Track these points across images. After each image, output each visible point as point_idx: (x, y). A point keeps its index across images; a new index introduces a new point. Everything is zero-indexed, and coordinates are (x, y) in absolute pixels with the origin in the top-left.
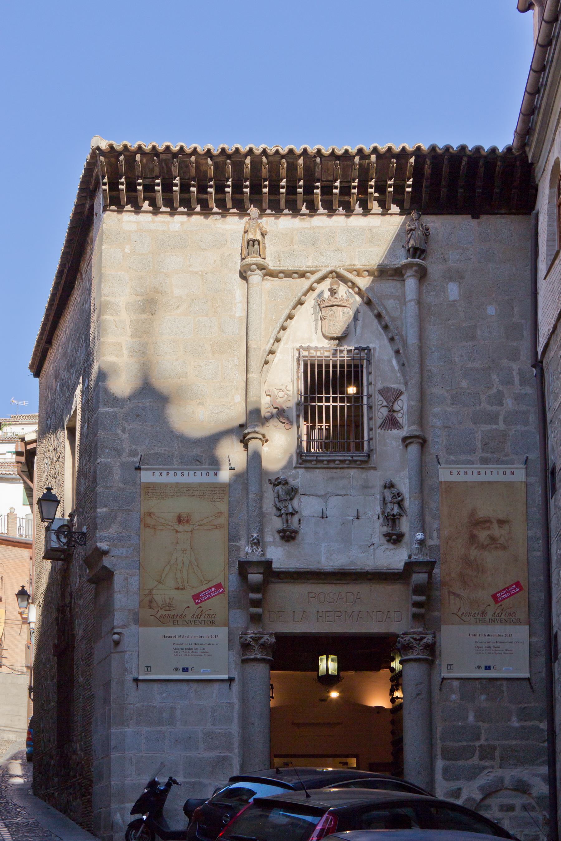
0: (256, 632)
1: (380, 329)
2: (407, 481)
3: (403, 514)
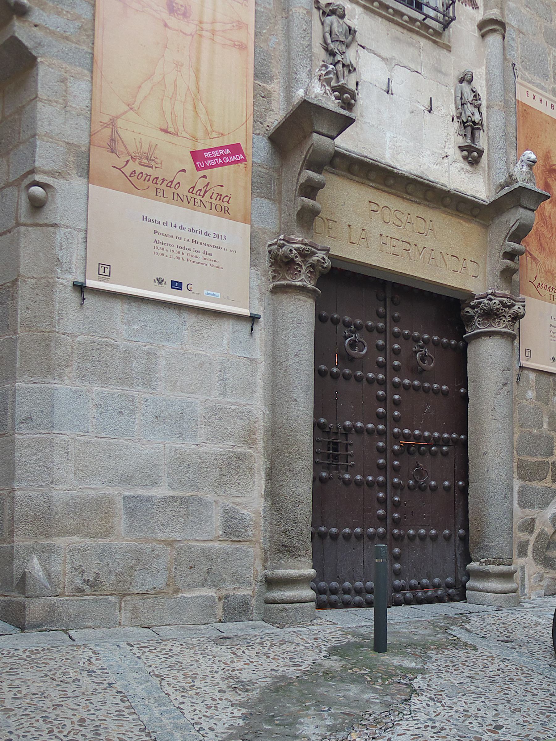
0: (306, 241)
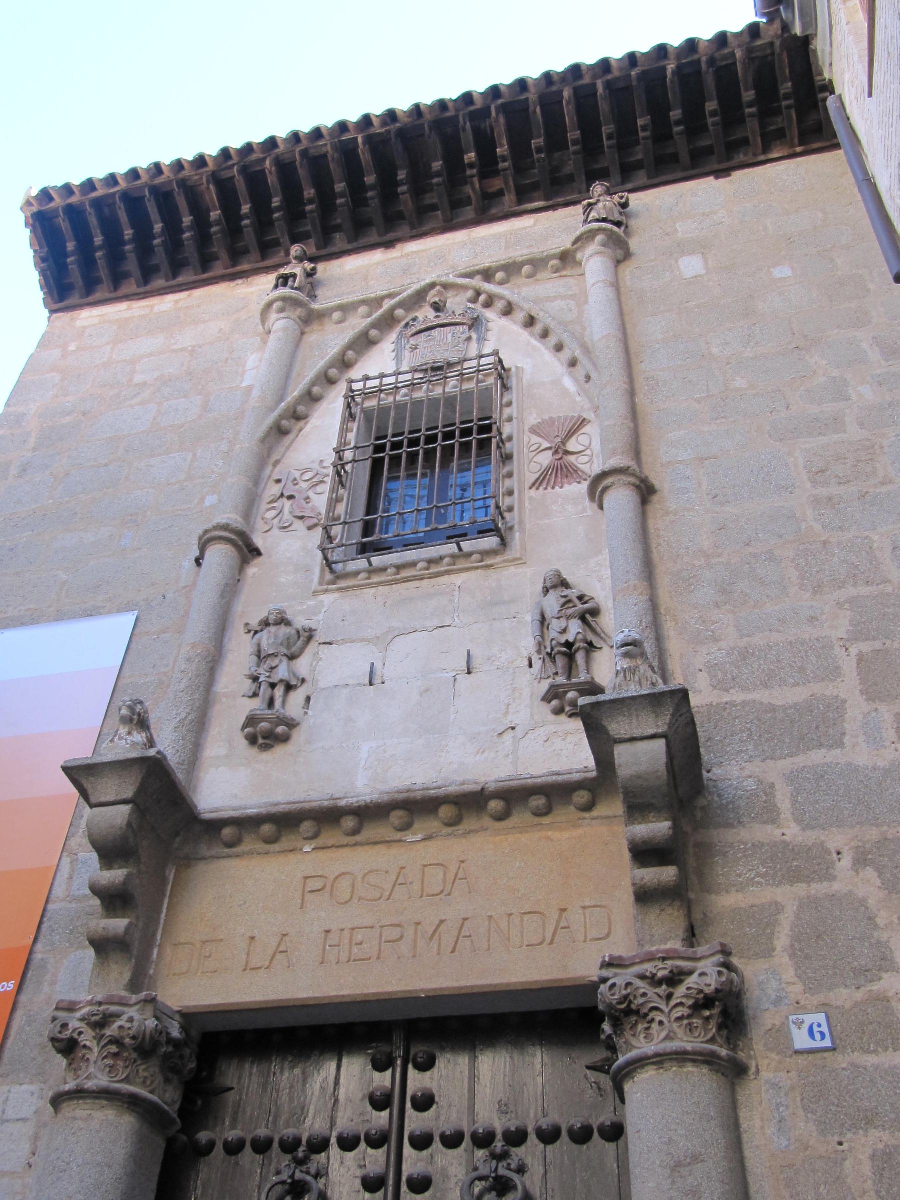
1: (535, 342)
2: (607, 573)
3: (596, 642)
